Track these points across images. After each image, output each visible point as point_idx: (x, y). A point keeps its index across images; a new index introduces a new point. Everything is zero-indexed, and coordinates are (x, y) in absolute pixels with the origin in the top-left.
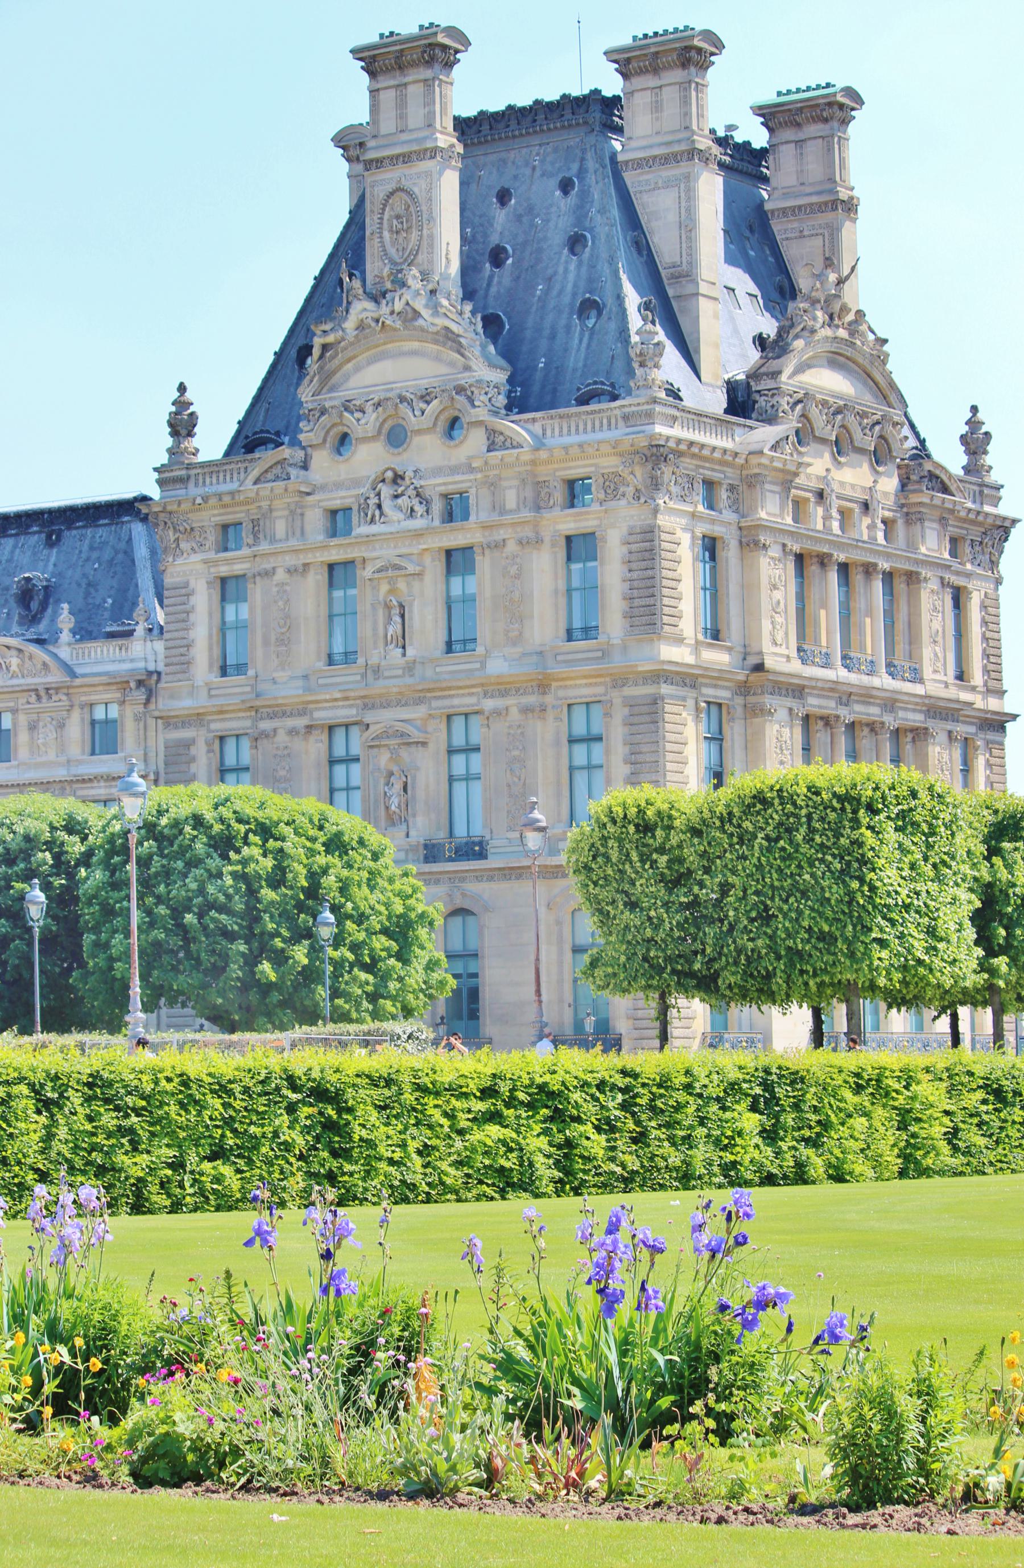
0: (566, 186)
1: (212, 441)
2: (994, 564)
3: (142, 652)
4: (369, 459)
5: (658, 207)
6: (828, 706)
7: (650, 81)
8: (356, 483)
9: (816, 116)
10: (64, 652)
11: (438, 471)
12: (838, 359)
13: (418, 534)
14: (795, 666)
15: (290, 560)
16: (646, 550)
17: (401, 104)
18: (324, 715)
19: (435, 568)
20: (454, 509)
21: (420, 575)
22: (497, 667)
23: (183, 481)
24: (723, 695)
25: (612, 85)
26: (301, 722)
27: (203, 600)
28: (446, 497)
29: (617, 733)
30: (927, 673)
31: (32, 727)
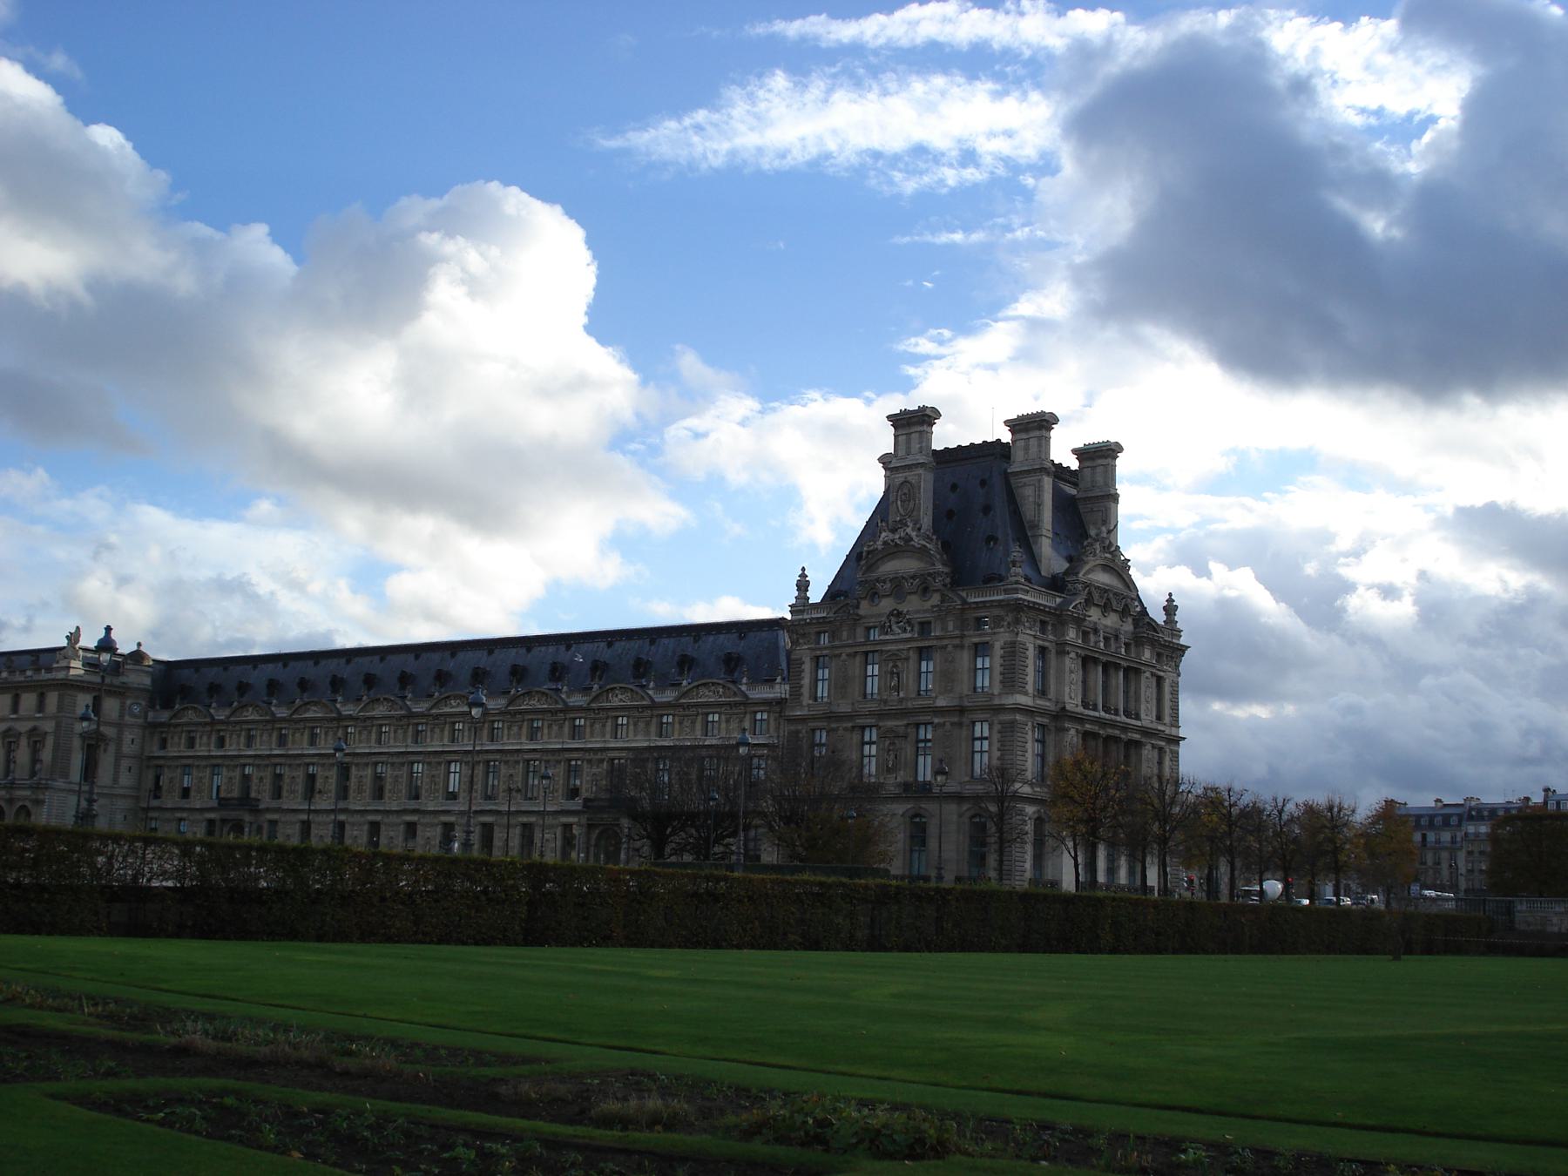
0: (983, 483)
1: (816, 595)
2: (1177, 666)
3: (780, 690)
4: (886, 605)
6: (1095, 728)
7: (1024, 436)
8: (880, 615)
9: (1100, 457)
10: (744, 688)
11: (918, 612)
12: (1107, 568)
14: (1080, 709)
15: (849, 650)
16: (1013, 652)
17: (908, 442)
18: (860, 722)
19: (913, 656)
20: (925, 627)
21: (907, 659)
22: (941, 702)
23: (802, 612)
24: (1045, 721)
25: (1006, 437)
27: (807, 667)
28: (921, 624)
30: (1143, 716)
31: (728, 721)
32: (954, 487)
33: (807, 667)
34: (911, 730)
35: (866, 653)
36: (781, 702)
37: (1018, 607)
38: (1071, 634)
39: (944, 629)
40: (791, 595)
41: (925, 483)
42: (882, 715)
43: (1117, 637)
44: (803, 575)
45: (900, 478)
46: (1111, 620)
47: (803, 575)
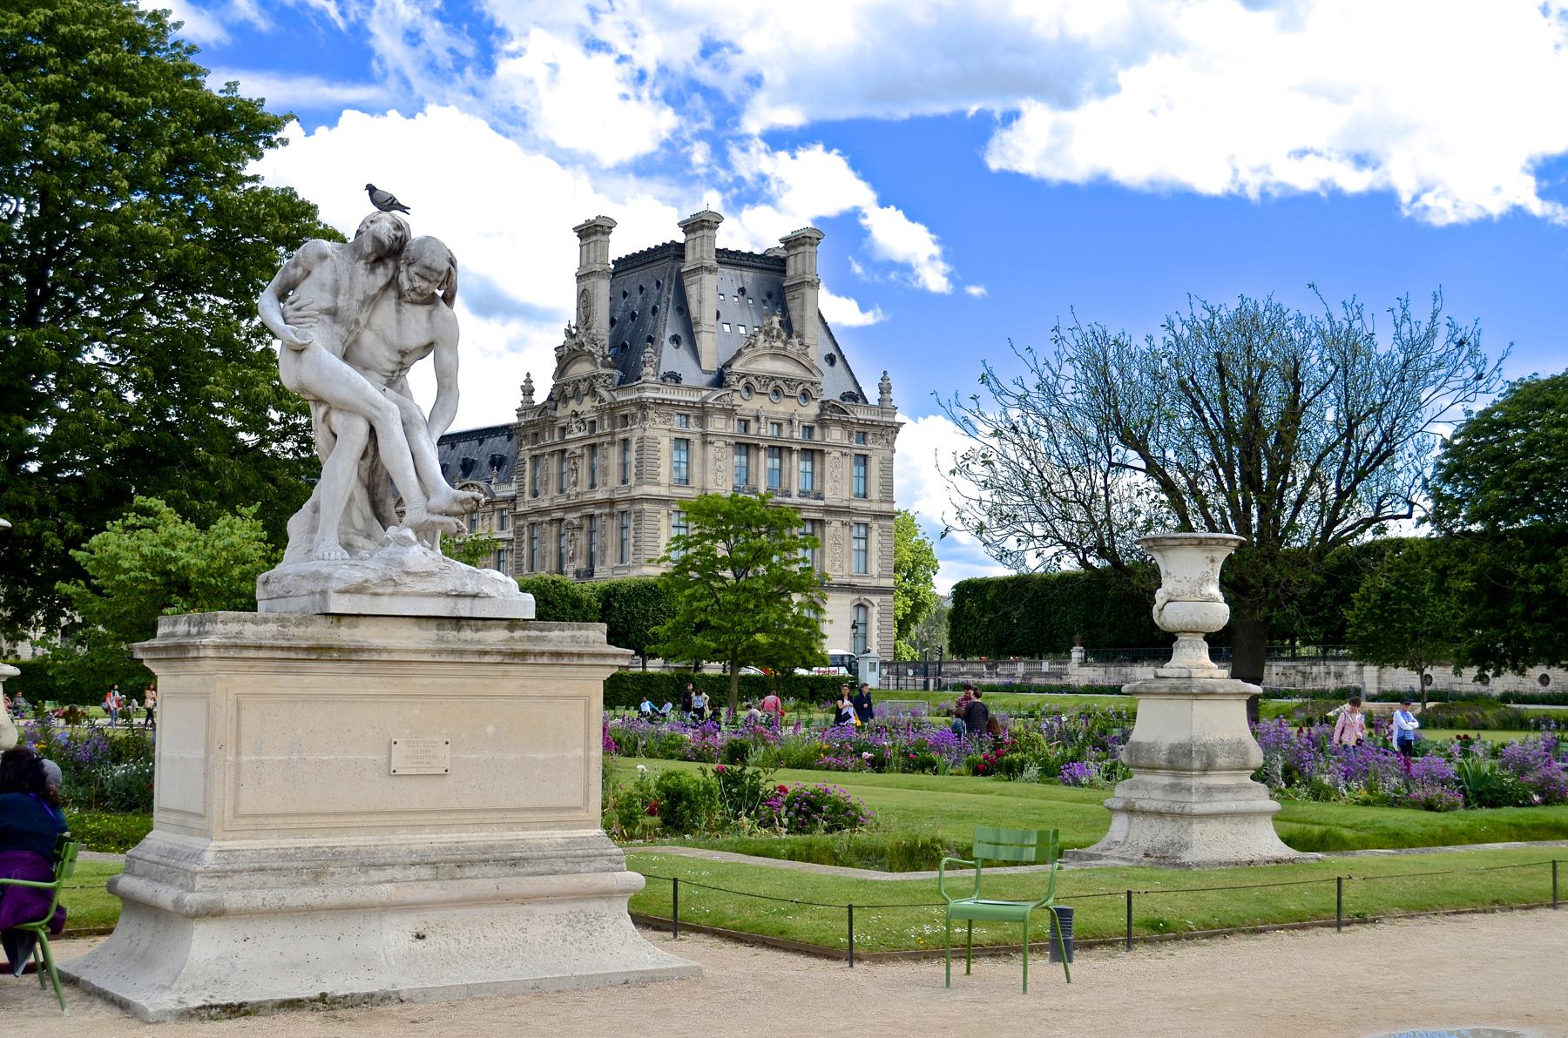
0: (658, 284)
1: (540, 397)
2: (890, 444)
4: (573, 405)
5: (692, 291)
13: (581, 439)
15: (549, 450)
21: (582, 456)
25: (680, 237)
27: (528, 466)
29: (632, 525)
32: (641, 289)
33: (528, 466)
34: (586, 524)
35: (563, 451)
36: (513, 499)
37: (642, 405)
38: (717, 424)
39: (602, 427)
40: (517, 399)
41: (602, 289)
42: (567, 509)
43: (791, 422)
44: (528, 381)
45: (587, 283)
46: (784, 408)
47: (528, 381)
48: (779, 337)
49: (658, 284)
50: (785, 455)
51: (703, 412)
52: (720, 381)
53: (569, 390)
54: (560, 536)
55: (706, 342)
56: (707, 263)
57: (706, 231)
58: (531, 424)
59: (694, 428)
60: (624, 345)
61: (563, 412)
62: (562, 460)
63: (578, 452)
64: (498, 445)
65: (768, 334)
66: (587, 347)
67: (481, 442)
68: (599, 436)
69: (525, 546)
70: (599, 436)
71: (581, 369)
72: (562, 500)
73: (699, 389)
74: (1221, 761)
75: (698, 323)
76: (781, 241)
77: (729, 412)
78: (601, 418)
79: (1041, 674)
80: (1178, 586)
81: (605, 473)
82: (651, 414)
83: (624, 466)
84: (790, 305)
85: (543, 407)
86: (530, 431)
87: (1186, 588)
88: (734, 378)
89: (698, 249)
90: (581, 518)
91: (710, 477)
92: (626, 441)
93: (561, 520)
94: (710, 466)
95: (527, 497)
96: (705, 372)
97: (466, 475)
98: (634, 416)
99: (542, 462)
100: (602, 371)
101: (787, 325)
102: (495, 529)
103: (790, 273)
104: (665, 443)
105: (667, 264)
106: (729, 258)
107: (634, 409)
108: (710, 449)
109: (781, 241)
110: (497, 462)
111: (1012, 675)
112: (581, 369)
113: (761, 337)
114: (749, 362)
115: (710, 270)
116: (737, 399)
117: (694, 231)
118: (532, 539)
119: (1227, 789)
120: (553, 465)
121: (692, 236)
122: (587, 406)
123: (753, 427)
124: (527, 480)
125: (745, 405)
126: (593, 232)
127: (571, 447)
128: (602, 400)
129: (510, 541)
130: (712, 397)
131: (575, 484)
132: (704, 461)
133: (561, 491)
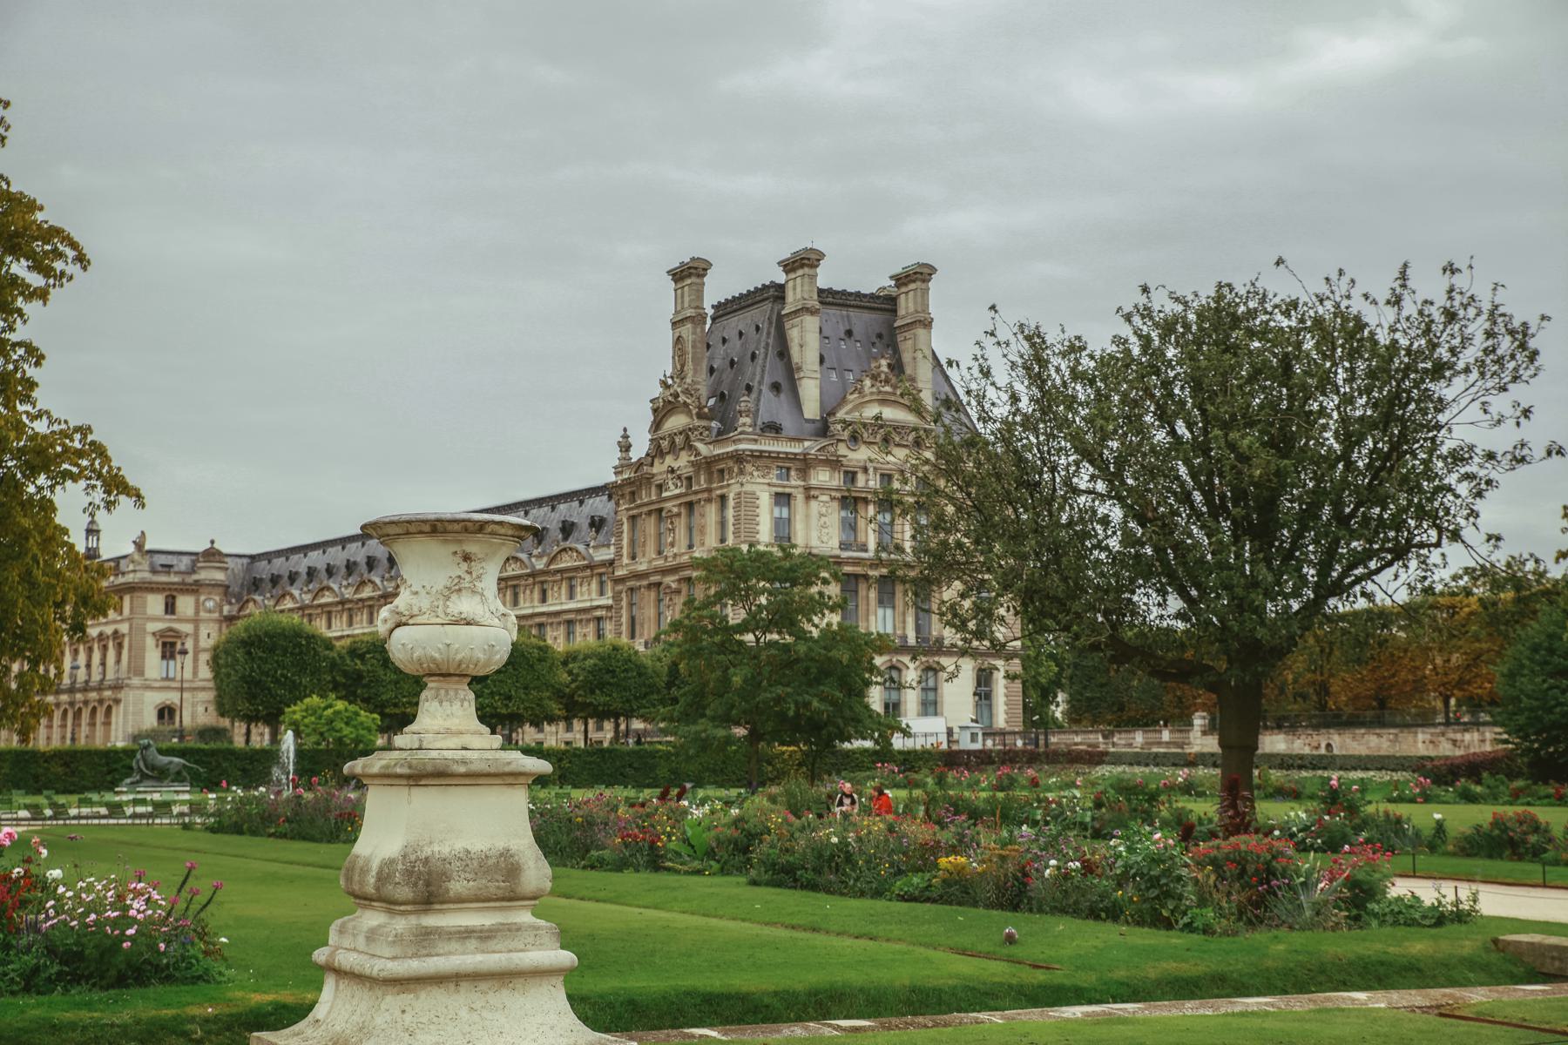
0: (758, 328)
1: (639, 451)
4: (669, 460)
5: (794, 334)
14: (837, 552)
15: (645, 509)
25: (780, 278)
26: (645, 583)
27: (625, 527)
32: (741, 334)
33: (625, 527)
35: (660, 510)
36: (611, 563)
40: (615, 457)
48: (887, 381)
49: (758, 328)
50: (860, 507)
51: (805, 464)
52: (823, 429)
53: (665, 444)
54: (660, 601)
55: (810, 392)
56: (810, 304)
57: (806, 270)
58: (628, 482)
59: (795, 481)
60: (722, 394)
61: (659, 468)
62: (660, 519)
63: (675, 510)
64: (600, 506)
65: (874, 378)
66: (682, 398)
67: (581, 502)
68: (696, 493)
69: (624, 612)
70: (696, 493)
71: (676, 422)
72: (660, 562)
73: (800, 440)
74: (457, 886)
75: (799, 369)
76: (891, 278)
77: (835, 464)
78: (697, 472)
79: (1160, 744)
80: (415, 601)
81: (702, 531)
82: (749, 468)
83: (723, 524)
84: (902, 346)
85: (640, 464)
86: (628, 490)
87: (425, 603)
88: (839, 427)
89: (799, 289)
90: (679, 581)
91: (814, 534)
92: (723, 498)
93: (659, 584)
94: (814, 521)
95: (625, 560)
96: (808, 421)
97: (565, 539)
98: (730, 470)
99: (639, 522)
100: (697, 422)
101: (897, 367)
102: (594, 596)
103: (902, 312)
104: (765, 499)
105: (767, 306)
106: (831, 298)
107: (731, 464)
108: (813, 503)
109: (891, 278)
110: (597, 524)
111: (1130, 745)
112: (676, 422)
113: (868, 382)
114: (855, 408)
115: (813, 312)
116: (842, 450)
117: (793, 270)
118: (631, 605)
119: (466, 934)
120: (650, 525)
121: (792, 276)
122: (682, 462)
123: (861, 478)
124: (625, 542)
125: (851, 455)
126: (689, 273)
127: (668, 505)
128: (698, 454)
129: (609, 608)
130: (811, 446)
131: (672, 545)
132: (807, 516)
133: (660, 553)
